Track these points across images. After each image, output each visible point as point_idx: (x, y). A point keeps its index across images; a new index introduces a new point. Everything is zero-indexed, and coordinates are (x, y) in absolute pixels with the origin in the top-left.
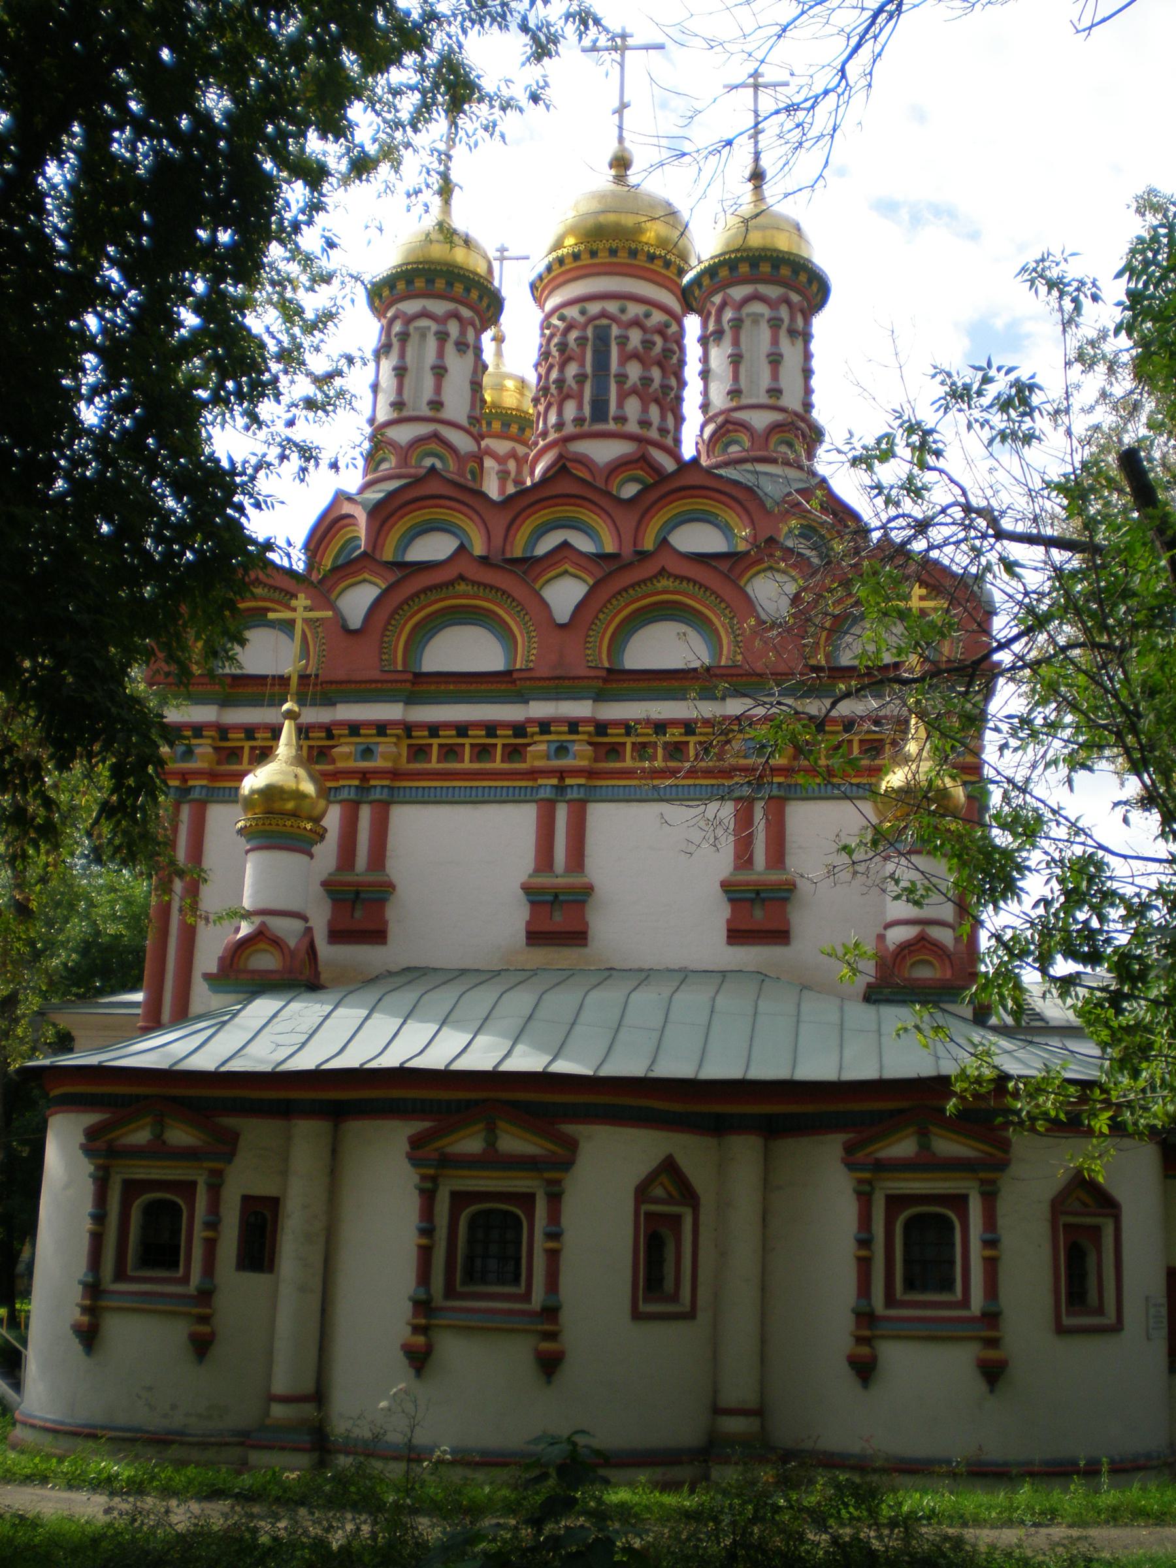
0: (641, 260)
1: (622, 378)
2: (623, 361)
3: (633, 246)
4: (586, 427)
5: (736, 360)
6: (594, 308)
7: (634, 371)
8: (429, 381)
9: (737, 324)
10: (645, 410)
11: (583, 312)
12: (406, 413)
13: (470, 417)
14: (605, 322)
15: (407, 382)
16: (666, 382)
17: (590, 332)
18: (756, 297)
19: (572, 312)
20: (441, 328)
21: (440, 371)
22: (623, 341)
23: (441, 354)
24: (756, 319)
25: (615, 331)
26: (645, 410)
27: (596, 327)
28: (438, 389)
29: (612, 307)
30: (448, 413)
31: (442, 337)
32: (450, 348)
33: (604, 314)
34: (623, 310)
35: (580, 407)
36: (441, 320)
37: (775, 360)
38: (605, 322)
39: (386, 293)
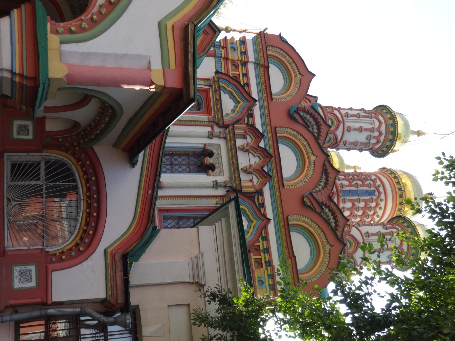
0: (399, 207)
1: (359, 201)
2: (364, 200)
3: (404, 204)
6: (381, 189)
7: (362, 205)
8: (357, 125)
10: (348, 209)
11: (379, 186)
12: (345, 118)
14: (377, 194)
15: (355, 118)
16: (358, 217)
19: (378, 183)
20: (375, 130)
21: (360, 130)
23: (366, 130)
25: (374, 197)
26: (348, 209)
27: (374, 191)
28: (355, 129)
29: (383, 196)
30: (346, 133)
32: (368, 133)
33: (380, 193)
34: (381, 200)
35: (347, 186)
36: (379, 130)
38: (377, 194)
39: (385, 111)
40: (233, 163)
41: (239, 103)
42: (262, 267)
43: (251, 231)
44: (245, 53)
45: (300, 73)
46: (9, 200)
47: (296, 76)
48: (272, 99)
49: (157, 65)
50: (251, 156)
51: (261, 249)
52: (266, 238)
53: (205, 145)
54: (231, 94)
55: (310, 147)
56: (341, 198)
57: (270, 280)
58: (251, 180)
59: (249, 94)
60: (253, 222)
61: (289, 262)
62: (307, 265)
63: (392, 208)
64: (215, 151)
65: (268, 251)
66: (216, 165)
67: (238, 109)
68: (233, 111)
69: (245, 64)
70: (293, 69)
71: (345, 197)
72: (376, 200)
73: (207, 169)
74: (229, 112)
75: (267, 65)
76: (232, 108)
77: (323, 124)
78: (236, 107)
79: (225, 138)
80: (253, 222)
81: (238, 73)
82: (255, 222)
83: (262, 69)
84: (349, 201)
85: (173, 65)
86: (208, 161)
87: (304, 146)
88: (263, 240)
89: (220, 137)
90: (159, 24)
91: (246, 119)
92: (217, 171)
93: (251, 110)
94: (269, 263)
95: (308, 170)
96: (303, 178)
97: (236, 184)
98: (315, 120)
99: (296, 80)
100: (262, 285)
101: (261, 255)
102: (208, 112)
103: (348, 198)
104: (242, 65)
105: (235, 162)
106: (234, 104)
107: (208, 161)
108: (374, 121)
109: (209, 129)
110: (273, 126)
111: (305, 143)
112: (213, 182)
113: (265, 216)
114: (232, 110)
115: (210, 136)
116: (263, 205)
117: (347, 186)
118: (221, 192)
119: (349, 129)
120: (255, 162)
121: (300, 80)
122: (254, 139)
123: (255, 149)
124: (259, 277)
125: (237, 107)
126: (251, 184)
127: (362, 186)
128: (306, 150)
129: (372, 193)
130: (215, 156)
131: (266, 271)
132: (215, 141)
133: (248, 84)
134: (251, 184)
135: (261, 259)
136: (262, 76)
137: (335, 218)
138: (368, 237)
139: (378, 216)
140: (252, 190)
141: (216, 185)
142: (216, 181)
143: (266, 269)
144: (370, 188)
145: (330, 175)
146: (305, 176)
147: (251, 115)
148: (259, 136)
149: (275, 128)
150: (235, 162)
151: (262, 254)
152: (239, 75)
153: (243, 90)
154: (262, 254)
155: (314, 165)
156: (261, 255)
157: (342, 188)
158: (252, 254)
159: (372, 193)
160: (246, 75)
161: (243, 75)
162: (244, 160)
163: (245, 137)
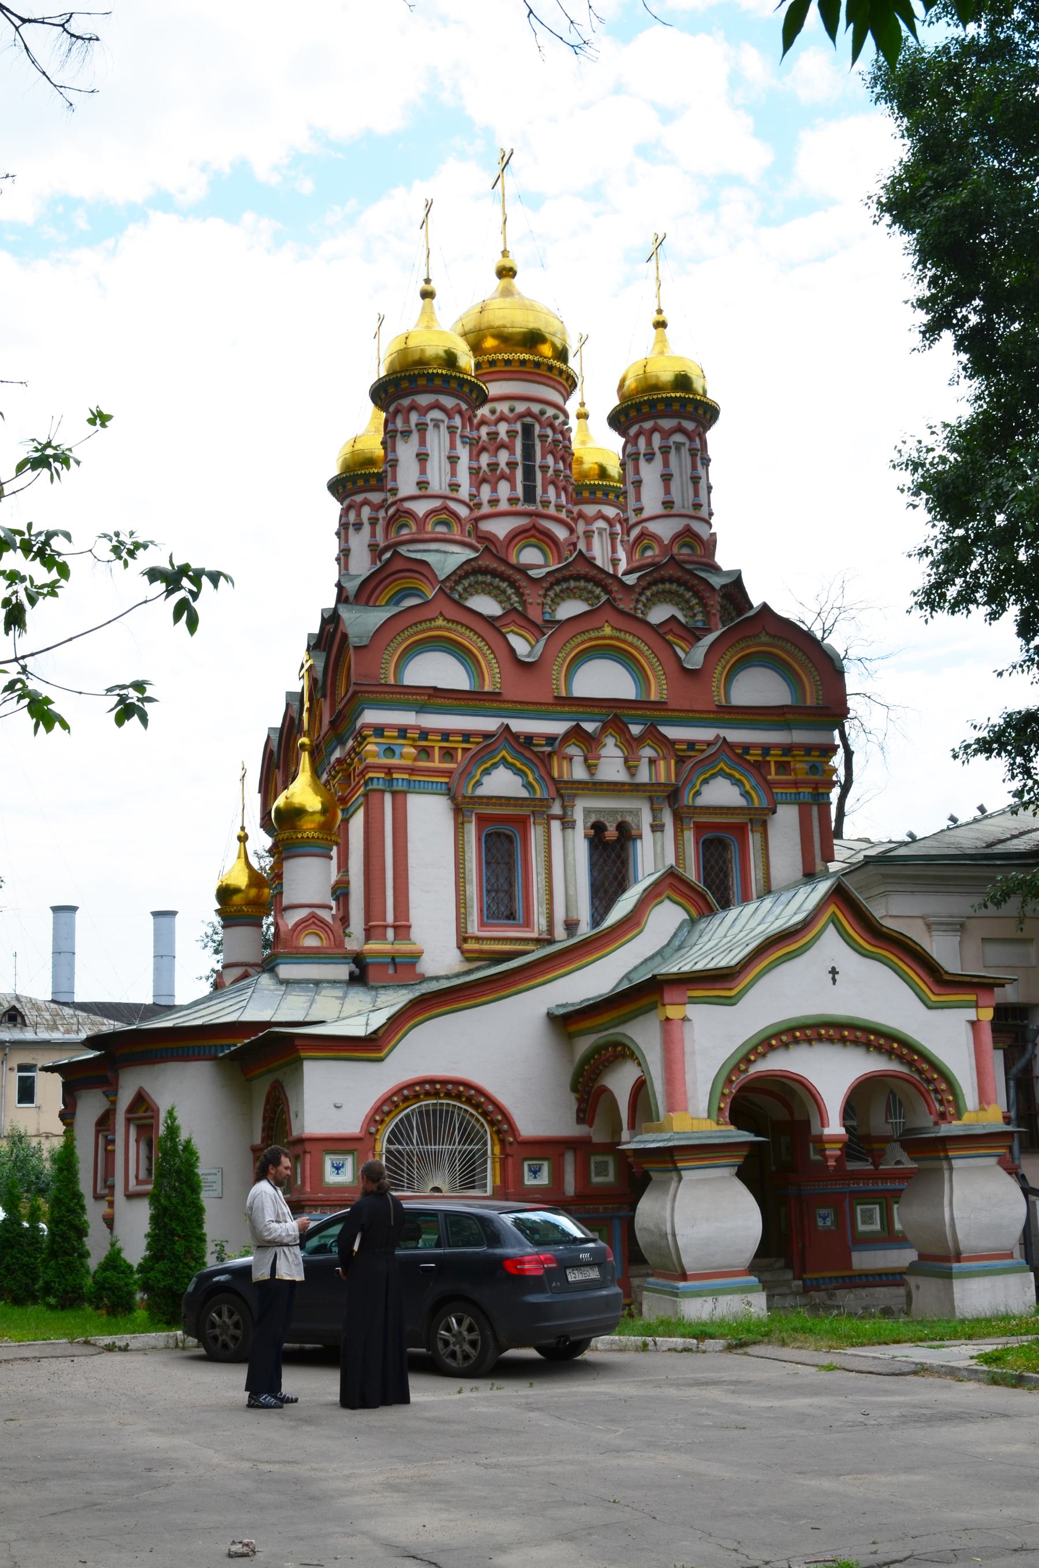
2: (544, 457)
4: (520, 507)
5: (666, 478)
6: (521, 407)
9: (665, 451)
11: (512, 410)
13: (470, 495)
14: (528, 420)
17: (518, 427)
18: (680, 430)
21: (453, 460)
22: (543, 437)
23: (453, 446)
24: (678, 446)
25: (537, 428)
26: (558, 496)
29: (536, 408)
31: (452, 430)
33: (529, 413)
34: (542, 413)
35: (513, 488)
37: (695, 480)
40: (625, 791)
41: (503, 758)
42: (789, 762)
43: (738, 776)
44: (403, 731)
45: (434, 619)
46: (898, 1162)
47: (439, 628)
48: (499, 694)
49: (971, 1014)
50: (603, 752)
51: (760, 759)
52: (746, 748)
53: (586, 836)
54: (487, 772)
55: (588, 631)
56: (540, 509)
57: (813, 753)
58: (652, 761)
59: (487, 736)
60: (721, 769)
61: (790, 717)
62: (785, 680)
63: (554, 388)
64: (593, 819)
65: (766, 749)
66: (620, 819)
67: (518, 764)
68: (518, 772)
69: (424, 734)
70: (424, 631)
71: (538, 498)
72: (542, 426)
73: (627, 835)
74: (518, 780)
75: (431, 692)
76: (509, 773)
77: (524, 584)
78: (510, 766)
79: (575, 796)
80: (721, 769)
81: (437, 750)
82: (722, 765)
83: (433, 701)
84: (545, 491)
85: (973, 997)
86: (611, 833)
87: (583, 642)
88: (748, 754)
89: (573, 806)
90: (929, 1008)
91: (536, 749)
92: (629, 819)
93: (516, 736)
94: (788, 749)
95: (631, 645)
96: (646, 657)
97: (662, 792)
98: (467, 575)
99: (449, 630)
100: (817, 768)
101: (769, 762)
102: (522, 823)
103: (539, 490)
104: (421, 739)
105: (626, 787)
106: (501, 768)
107: (611, 833)
108: (432, 420)
109: (556, 825)
110: (551, 701)
111: (579, 639)
112: (653, 831)
113: (709, 744)
114: (515, 774)
115: (567, 824)
116: (691, 745)
117: (513, 488)
118: (667, 819)
119: (454, 487)
120: (616, 745)
121: (449, 621)
122: (573, 740)
123: (590, 742)
124: (807, 773)
125: (514, 765)
126: (662, 764)
127: (511, 450)
128: (591, 639)
129: (527, 430)
130: (602, 819)
131: (798, 758)
132: (578, 815)
133: (467, 736)
134: (662, 764)
135: (776, 762)
136: (447, 702)
137: (663, 581)
138: (673, 502)
139: (556, 417)
140: (673, 762)
141: (657, 828)
142: (652, 826)
143: (794, 756)
144: (517, 432)
145: (582, 572)
146: (641, 653)
147: (529, 739)
148: (576, 734)
149: (556, 698)
150: (626, 787)
151: (768, 759)
152: (441, 748)
153: (486, 749)
154: (768, 759)
155: (621, 631)
156: (769, 762)
157: (518, 500)
158: (769, 777)
159: (527, 430)
160: (446, 735)
161: (443, 740)
162: (612, 765)
163: (570, 759)
